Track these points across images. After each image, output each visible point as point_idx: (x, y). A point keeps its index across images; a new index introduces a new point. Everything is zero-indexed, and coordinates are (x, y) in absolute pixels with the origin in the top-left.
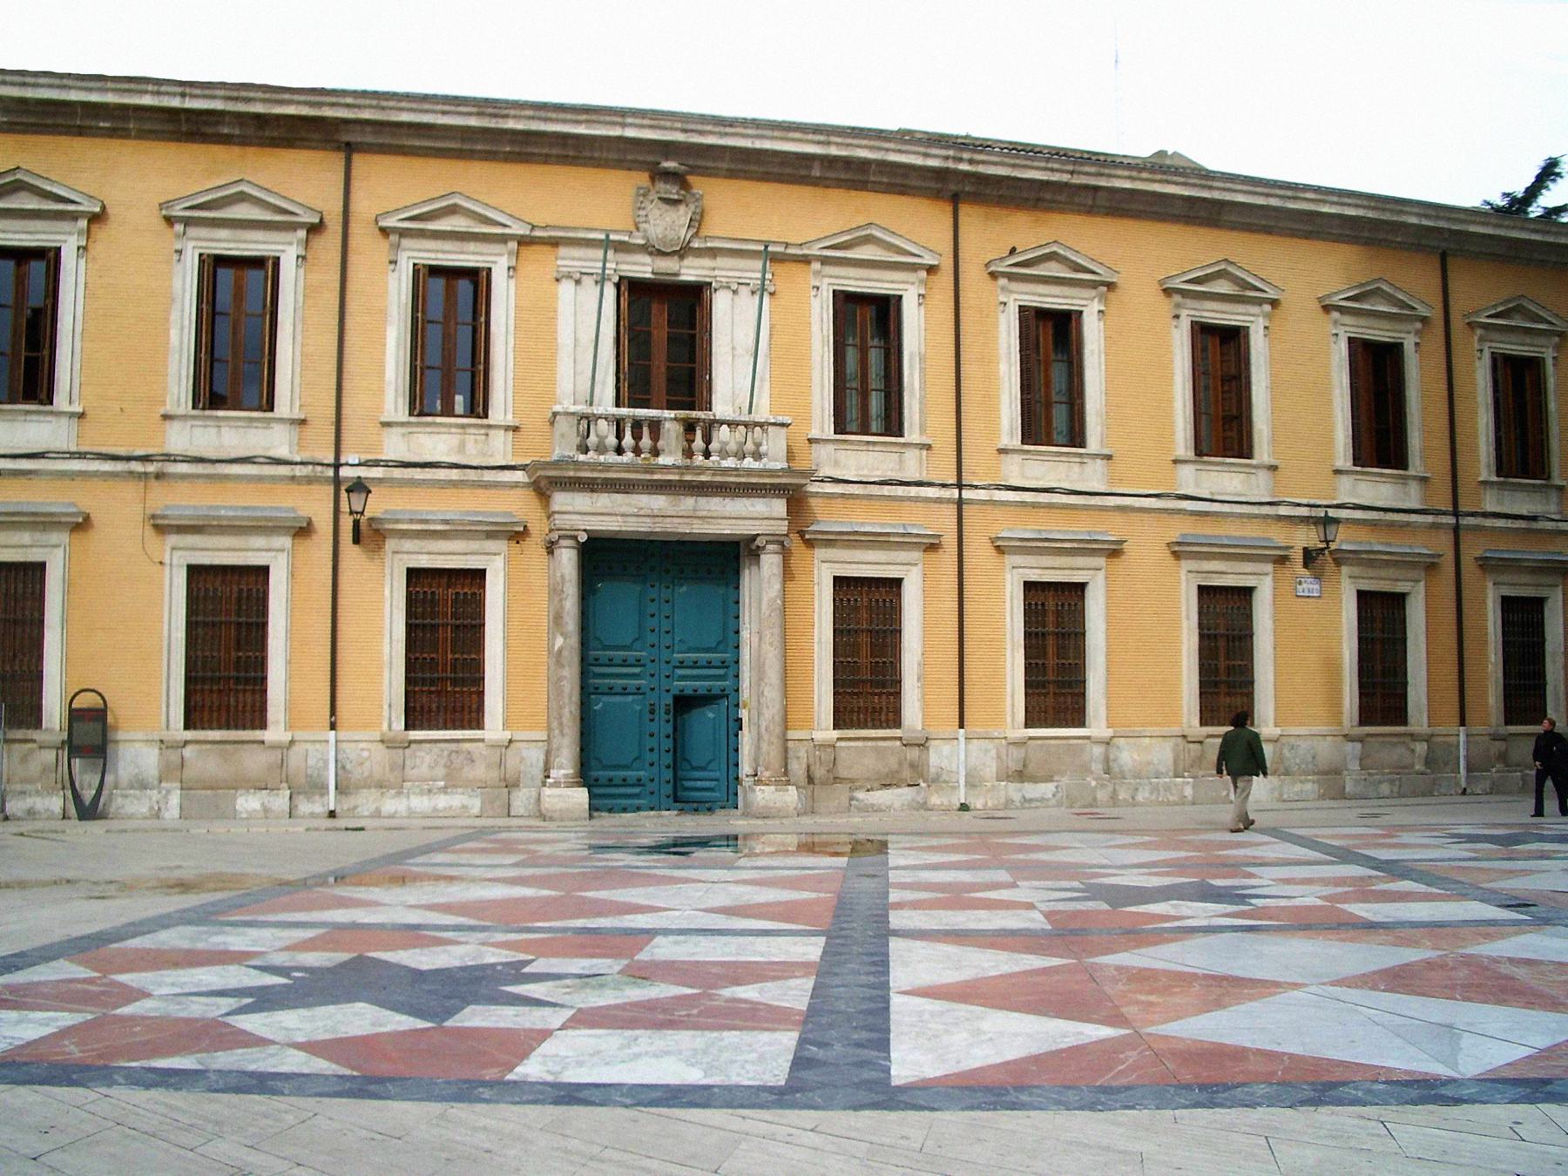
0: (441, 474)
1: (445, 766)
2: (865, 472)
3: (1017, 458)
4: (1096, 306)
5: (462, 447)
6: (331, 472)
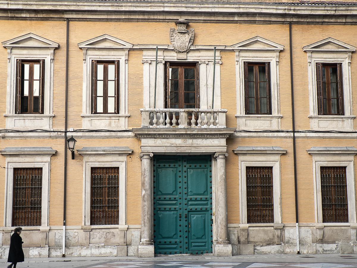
0: (103, 134)
2: (257, 128)
3: (316, 120)
4: (347, 61)
5: (110, 124)
6: (63, 134)
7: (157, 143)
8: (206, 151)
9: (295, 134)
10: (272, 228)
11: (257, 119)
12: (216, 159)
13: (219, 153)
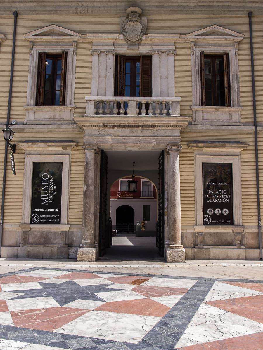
1: (45, 238)
9: (258, 127)
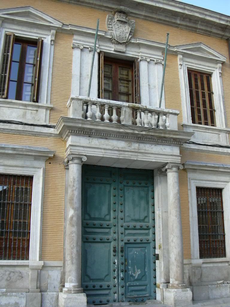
0: (13, 127)
1: (7, 280)
2: (206, 141)
5: (24, 115)
7: (93, 143)
8: (156, 161)
10: (227, 264)
11: (205, 131)
12: (164, 174)
13: (172, 165)
